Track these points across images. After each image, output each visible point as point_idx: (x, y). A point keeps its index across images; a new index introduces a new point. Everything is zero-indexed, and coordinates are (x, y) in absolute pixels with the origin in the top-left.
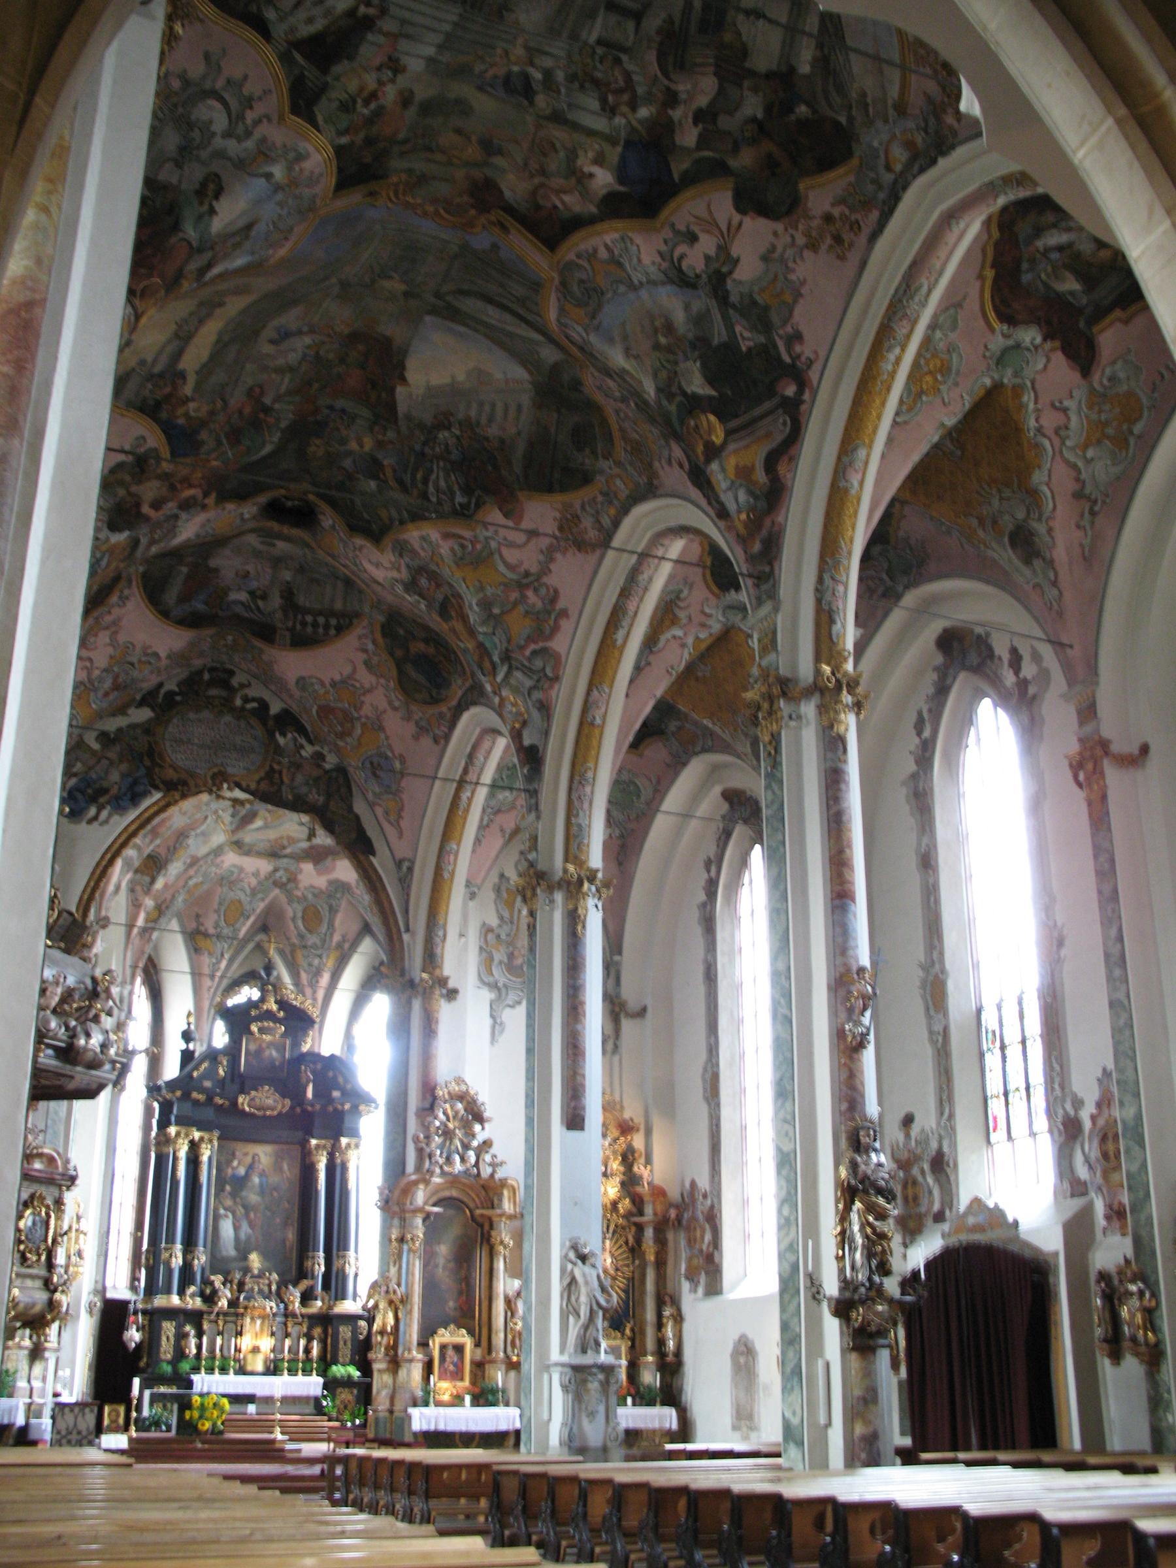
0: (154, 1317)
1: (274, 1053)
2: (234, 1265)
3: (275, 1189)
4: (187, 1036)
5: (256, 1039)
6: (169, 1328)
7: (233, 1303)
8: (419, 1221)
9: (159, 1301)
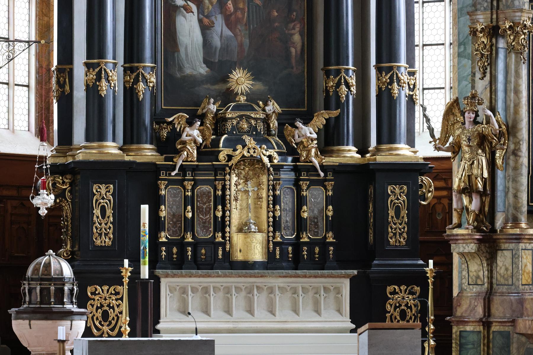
0: (77, 177)
2: (202, 89)
6: (103, 193)
7: (208, 152)
9: (84, 151)
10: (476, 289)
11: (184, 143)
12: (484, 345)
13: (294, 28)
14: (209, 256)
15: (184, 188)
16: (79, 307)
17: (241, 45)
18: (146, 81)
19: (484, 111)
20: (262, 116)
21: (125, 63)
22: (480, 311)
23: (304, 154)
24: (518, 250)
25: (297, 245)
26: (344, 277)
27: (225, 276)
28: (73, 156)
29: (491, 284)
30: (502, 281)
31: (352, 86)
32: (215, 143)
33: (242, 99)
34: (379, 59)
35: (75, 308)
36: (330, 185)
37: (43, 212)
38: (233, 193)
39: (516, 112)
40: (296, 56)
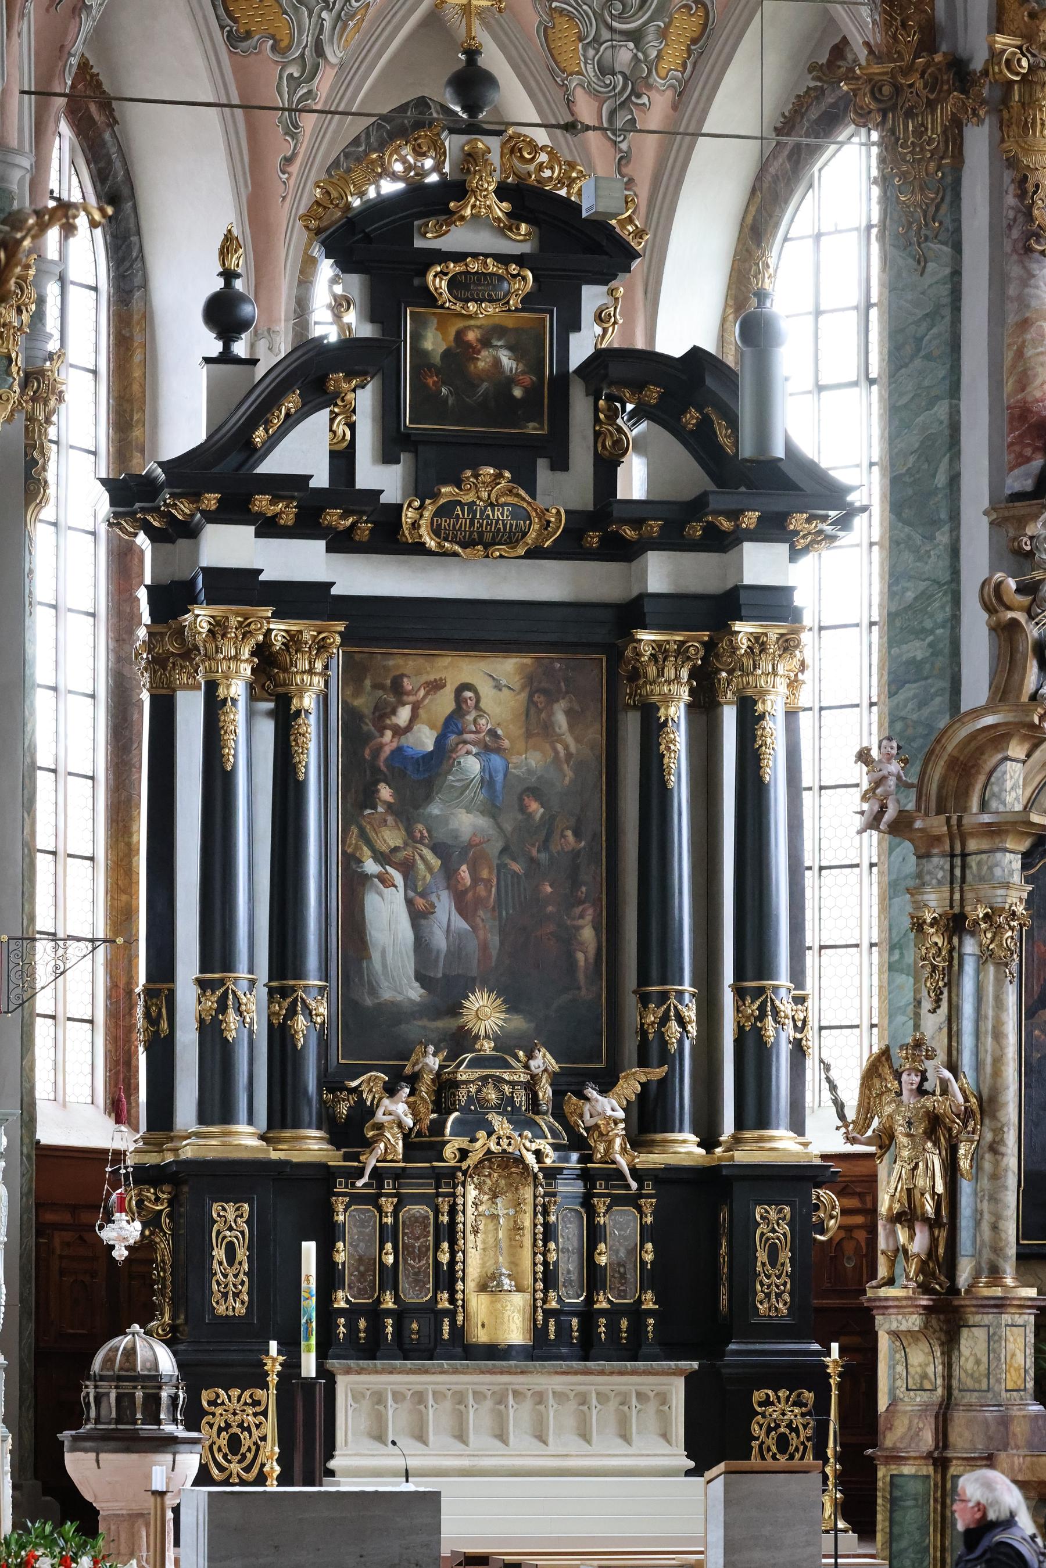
0: (185, 1189)
1: (507, 360)
2: (413, 1029)
3: (534, 792)
4: (224, 314)
5: (447, 317)
6: (231, 1219)
7: (422, 1144)
8: (1010, 863)
9: (195, 1142)
10: (920, 1398)
11: (380, 1127)
12: (935, 1500)
13: (582, 916)
14: (425, 1334)
15: (380, 1209)
16: (188, 1429)
17: (484, 947)
18: (309, 1013)
19: (937, 1070)
20: (524, 1078)
21: (270, 979)
22: (928, 1439)
23: (601, 1148)
24: (999, 1326)
25: (588, 1315)
26: (676, 1373)
27: (456, 1372)
28: (175, 1150)
29: (949, 1388)
30: (970, 1383)
31: (690, 1022)
32: (437, 1128)
33: (487, 1046)
34: (739, 974)
35: (180, 1431)
36: (648, 1205)
37: (120, 1253)
38: (470, 1218)
39: (997, 1073)
40: (586, 968)
